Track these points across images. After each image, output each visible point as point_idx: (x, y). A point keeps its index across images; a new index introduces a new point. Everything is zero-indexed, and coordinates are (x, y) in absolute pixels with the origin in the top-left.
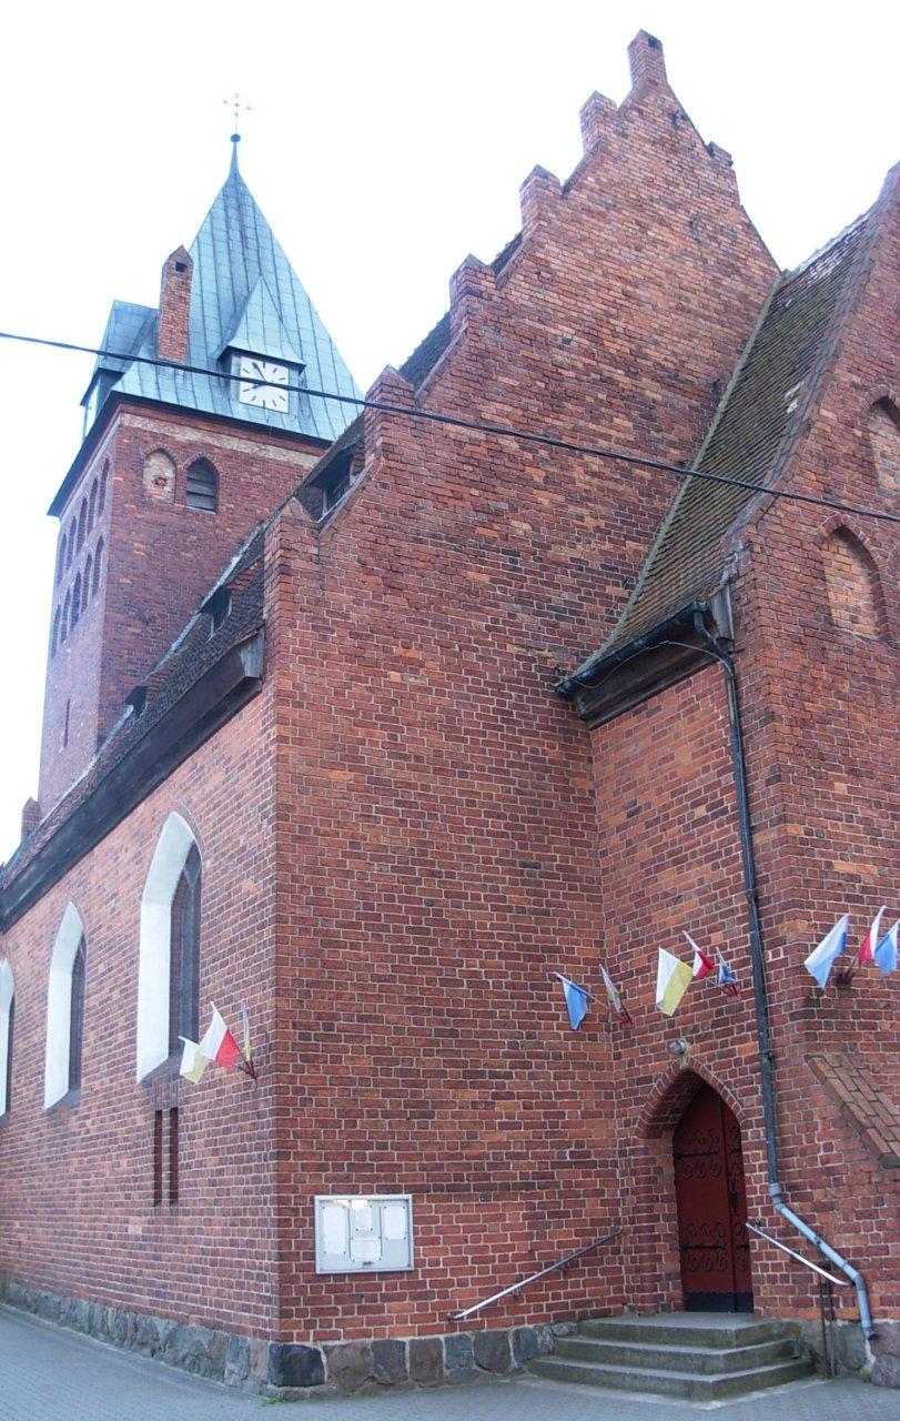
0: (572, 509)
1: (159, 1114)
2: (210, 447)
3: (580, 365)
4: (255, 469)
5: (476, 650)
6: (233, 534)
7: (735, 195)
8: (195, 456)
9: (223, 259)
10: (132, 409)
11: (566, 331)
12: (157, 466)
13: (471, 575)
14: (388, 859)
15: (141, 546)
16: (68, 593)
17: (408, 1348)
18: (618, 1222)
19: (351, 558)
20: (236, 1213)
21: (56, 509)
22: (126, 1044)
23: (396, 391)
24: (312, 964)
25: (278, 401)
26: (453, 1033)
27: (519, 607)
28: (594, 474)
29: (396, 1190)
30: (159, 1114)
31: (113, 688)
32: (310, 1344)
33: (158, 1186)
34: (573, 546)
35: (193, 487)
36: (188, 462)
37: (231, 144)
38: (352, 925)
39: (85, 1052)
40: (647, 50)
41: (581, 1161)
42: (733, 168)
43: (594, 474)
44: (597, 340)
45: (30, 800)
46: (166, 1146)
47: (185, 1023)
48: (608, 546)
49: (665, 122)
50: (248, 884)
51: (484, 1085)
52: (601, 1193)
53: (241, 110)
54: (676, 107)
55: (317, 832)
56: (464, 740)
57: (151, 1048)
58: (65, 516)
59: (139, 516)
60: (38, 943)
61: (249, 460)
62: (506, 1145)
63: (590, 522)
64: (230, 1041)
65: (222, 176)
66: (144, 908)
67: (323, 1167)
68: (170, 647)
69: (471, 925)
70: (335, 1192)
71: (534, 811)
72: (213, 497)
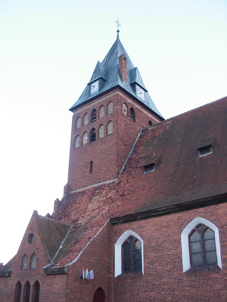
6: (139, 128)
10: (120, 90)
21: (72, 110)
37: (117, 33)
53: (119, 25)
61: (140, 111)
68: (129, 153)
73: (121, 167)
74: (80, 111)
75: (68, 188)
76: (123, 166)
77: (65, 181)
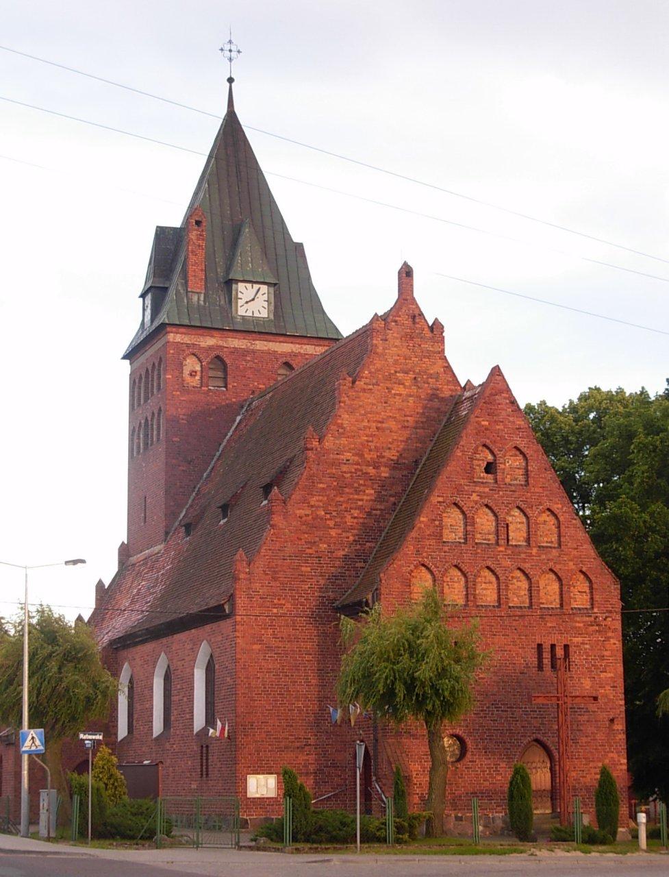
0: (344, 534)
1: (202, 746)
2: (221, 347)
3: (353, 470)
4: (248, 358)
5: (304, 597)
8: (213, 354)
9: (227, 201)
11: (348, 455)
12: (191, 364)
13: (303, 569)
14: (271, 672)
15: (184, 417)
16: (140, 423)
17: (274, 820)
18: (346, 785)
20: (226, 780)
21: (130, 355)
22: (190, 719)
23: (278, 501)
24: (247, 707)
25: (262, 310)
26: (292, 726)
27: (321, 578)
28: (355, 518)
29: (272, 774)
30: (202, 746)
31: (172, 504)
32: (245, 817)
33: (202, 771)
34: (344, 550)
35: (211, 373)
36: (209, 360)
37: (228, 84)
38: (259, 694)
40: (406, 274)
41: (334, 766)
42: (444, 334)
43: (355, 518)
44: (362, 456)
45: (123, 543)
46: (204, 758)
48: (358, 547)
49: (409, 322)
50: (228, 679)
51: (301, 742)
52: (341, 776)
53: (234, 54)
54: (417, 313)
55: (249, 665)
56: (298, 630)
57: (199, 721)
59: (182, 399)
60: (146, 662)
61: (244, 353)
62: (308, 760)
63: (351, 538)
64: (223, 729)
65: (223, 111)
66: (195, 670)
67: (250, 767)
68: (202, 476)
69: (298, 691)
70: (253, 774)
71: (323, 651)
72: (225, 379)
74: (142, 359)
76: (179, 514)
77: (122, 536)
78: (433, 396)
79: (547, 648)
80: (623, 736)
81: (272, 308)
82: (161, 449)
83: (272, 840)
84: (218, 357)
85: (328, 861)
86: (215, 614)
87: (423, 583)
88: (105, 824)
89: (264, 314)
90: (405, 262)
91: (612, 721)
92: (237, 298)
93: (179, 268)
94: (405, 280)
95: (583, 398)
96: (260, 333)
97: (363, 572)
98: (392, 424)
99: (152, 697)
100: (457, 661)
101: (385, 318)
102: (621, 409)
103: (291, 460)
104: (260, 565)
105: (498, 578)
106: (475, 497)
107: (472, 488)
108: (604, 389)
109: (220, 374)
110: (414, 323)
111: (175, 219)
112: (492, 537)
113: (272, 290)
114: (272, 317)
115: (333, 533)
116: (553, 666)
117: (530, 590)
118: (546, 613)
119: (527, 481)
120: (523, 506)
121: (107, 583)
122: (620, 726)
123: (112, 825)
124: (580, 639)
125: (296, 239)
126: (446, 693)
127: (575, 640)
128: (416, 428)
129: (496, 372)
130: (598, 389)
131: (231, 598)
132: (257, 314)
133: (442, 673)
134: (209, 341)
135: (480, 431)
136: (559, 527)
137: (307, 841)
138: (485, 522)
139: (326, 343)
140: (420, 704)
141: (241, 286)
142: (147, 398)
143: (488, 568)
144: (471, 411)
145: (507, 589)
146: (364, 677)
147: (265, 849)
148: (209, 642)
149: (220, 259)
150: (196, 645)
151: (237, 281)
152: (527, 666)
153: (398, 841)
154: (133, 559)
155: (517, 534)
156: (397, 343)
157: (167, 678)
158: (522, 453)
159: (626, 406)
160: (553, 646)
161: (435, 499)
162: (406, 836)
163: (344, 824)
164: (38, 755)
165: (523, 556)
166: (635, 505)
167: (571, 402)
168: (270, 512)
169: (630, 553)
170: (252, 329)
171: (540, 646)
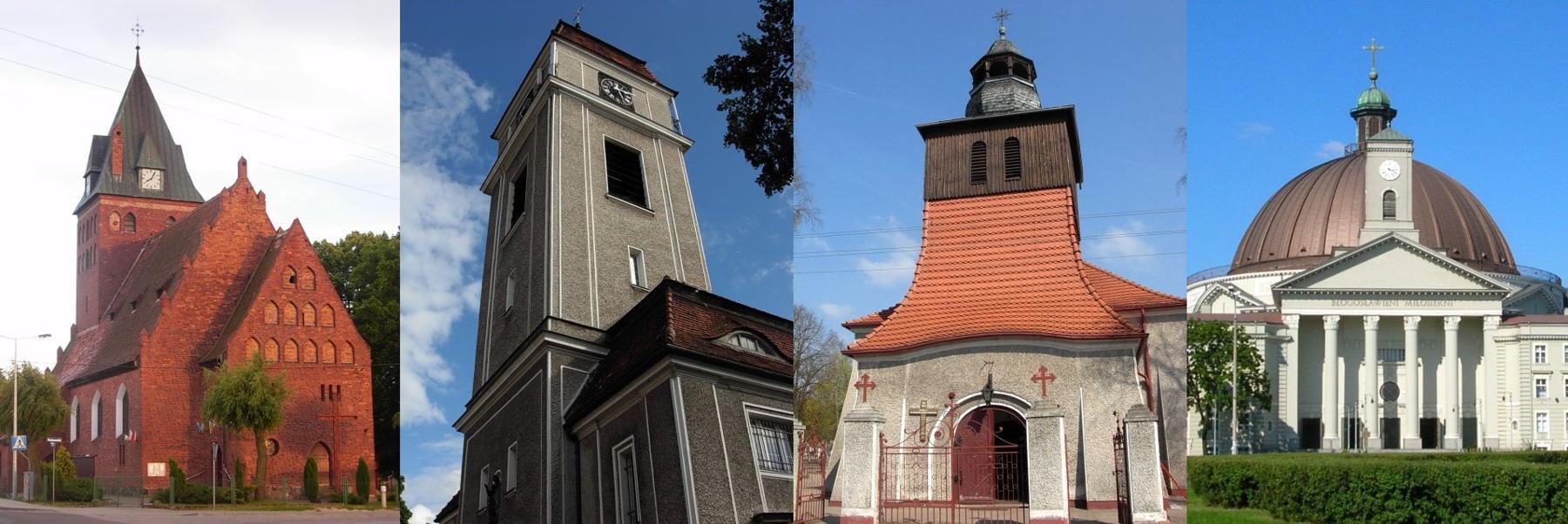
2: (132, 207)
7: (265, 210)
8: (127, 212)
11: (208, 272)
12: (114, 217)
19: (155, 341)
21: (78, 212)
35: (126, 223)
39: (103, 429)
40: (243, 164)
44: (216, 272)
47: (126, 431)
49: (244, 193)
57: (119, 430)
58: (82, 217)
61: (146, 211)
63: (210, 322)
64: (133, 435)
65: (133, 66)
66: (117, 401)
72: (134, 226)
73: (105, 308)
74: (85, 215)
75: (75, 330)
77: (73, 321)
78: (259, 237)
79: (327, 387)
80: (372, 440)
81: (163, 183)
82: (95, 269)
83: (163, 502)
84: (130, 213)
85: (197, 514)
86: (129, 367)
87: (253, 348)
88: (63, 492)
89: (158, 188)
90: (242, 157)
91: (366, 431)
92: (142, 178)
93: (107, 160)
94: (242, 167)
95: (348, 238)
96: (156, 199)
97: (217, 342)
98: (234, 253)
99: (90, 418)
100: (273, 395)
101: (230, 190)
102: (371, 245)
103: (174, 275)
104: (155, 338)
105: (297, 345)
106: (283, 297)
107: (282, 291)
108: (361, 232)
109: (132, 224)
110: (248, 193)
111: (105, 131)
112: (294, 321)
113: (162, 173)
114: (162, 189)
115: (199, 318)
116: (331, 398)
117: (317, 352)
118: (326, 367)
119: (315, 287)
120: (312, 302)
121: (64, 349)
122: (371, 434)
123: (67, 493)
124: (347, 382)
125: (177, 143)
126: (267, 414)
127: (343, 382)
128: (249, 256)
129: (296, 222)
130: (357, 233)
131: (138, 357)
132: (153, 188)
133: (264, 402)
134: (125, 204)
135: (287, 258)
136: (334, 315)
137: (183, 502)
138: (290, 312)
139: (195, 205)
140: (251, 420)
141: (144, 171)
142: (87, 238)
143: (292, 339)
144: (282, 246)
145: (303, 352)
146: (217, 404)
147: (158, 507)
148: (125, 384)
149: (131, 155)
150: (117, 385)
151: (142, 168)
152: (315, 399)
153: (238, 503)
154: (80, 334)
155: (309, 319)
156: (238, 205)
157: (100, 405)
158: (312, 271)
159: (374, 243)
160: (330, 386)
161: (260, 298)
162: (243, 500)
163: (205, 492)
164: (23, 451)
165: (313, 332)
166: (379, 302)
167: (341, 240)
168: (162, 306)
169: (376, 330)
170: (150, 197)
171: (323, 386)
